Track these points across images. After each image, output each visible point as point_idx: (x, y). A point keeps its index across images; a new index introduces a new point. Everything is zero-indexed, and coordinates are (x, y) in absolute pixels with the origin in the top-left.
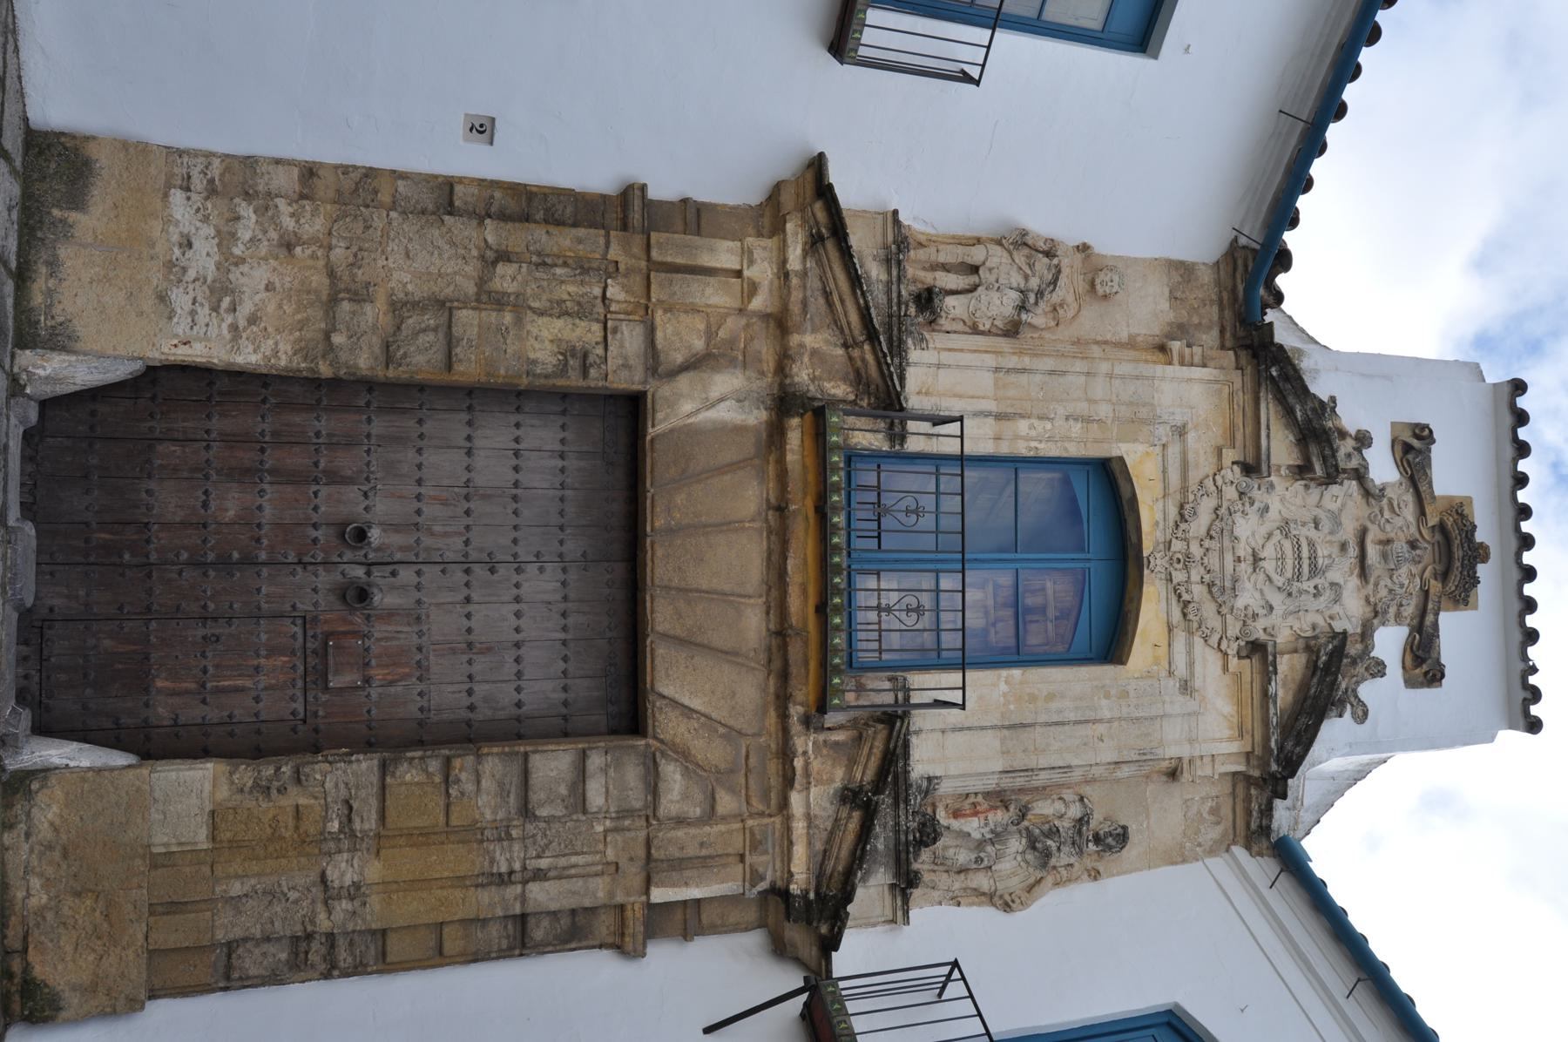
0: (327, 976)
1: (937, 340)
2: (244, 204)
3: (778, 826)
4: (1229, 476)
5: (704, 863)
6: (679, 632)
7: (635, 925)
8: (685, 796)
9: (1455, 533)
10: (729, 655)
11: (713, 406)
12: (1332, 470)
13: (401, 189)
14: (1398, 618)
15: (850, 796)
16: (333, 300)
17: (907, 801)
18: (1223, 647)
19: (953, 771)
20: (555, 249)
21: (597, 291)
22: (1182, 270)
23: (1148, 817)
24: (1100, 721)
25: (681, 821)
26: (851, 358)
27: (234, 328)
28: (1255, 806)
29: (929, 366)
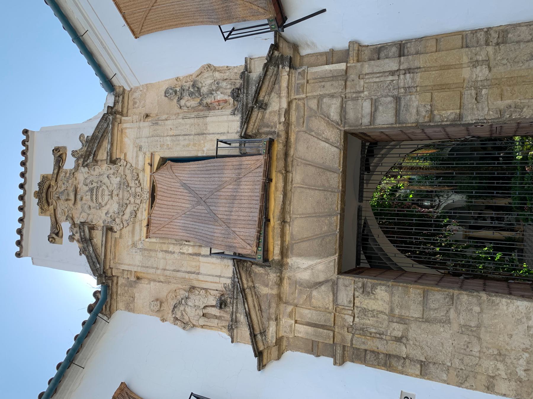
0: (489, 29)
1: (220, 287)
2: (522, 377)
3: (293, 94)
4: (118, 227)
5: (323, 79)
6: (328, 173)
7: (353, 54)
8: (329, 106)
9: (44, 202)
10: (308, 163)
11: (310, 266)
12: (82, 227)
13: (445, 375)
15: (263, 106)
16: (478, 327)
18: (125, 163)
19: (225, 118)
20: (375, 340)
21: (357, 320)
22: (129, 308)
23: (158, 100)
24: (171, 136)
25: (332, 96)
26: (253, 282)
28: (120, 104)
29: (224, 277)
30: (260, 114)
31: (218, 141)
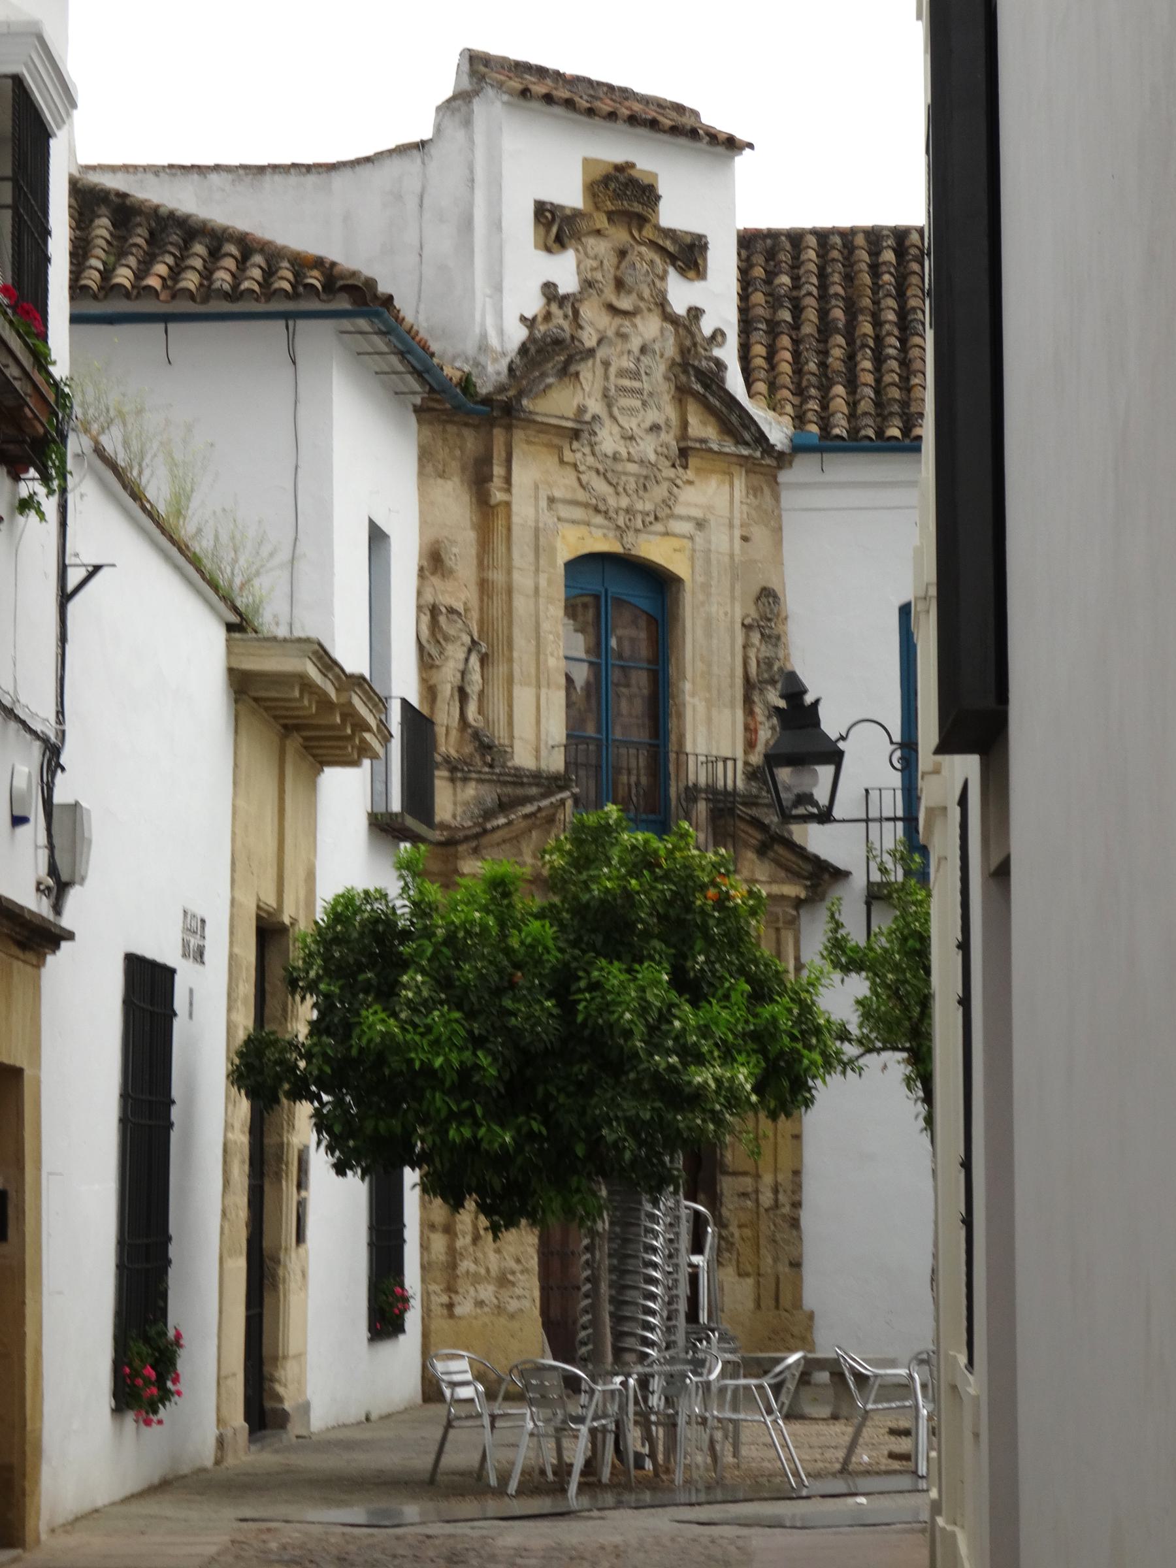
14: (663, 278)
17: (757, 797)
27: (522, 1272)
30: (754, 842)
31: (735, 760)
